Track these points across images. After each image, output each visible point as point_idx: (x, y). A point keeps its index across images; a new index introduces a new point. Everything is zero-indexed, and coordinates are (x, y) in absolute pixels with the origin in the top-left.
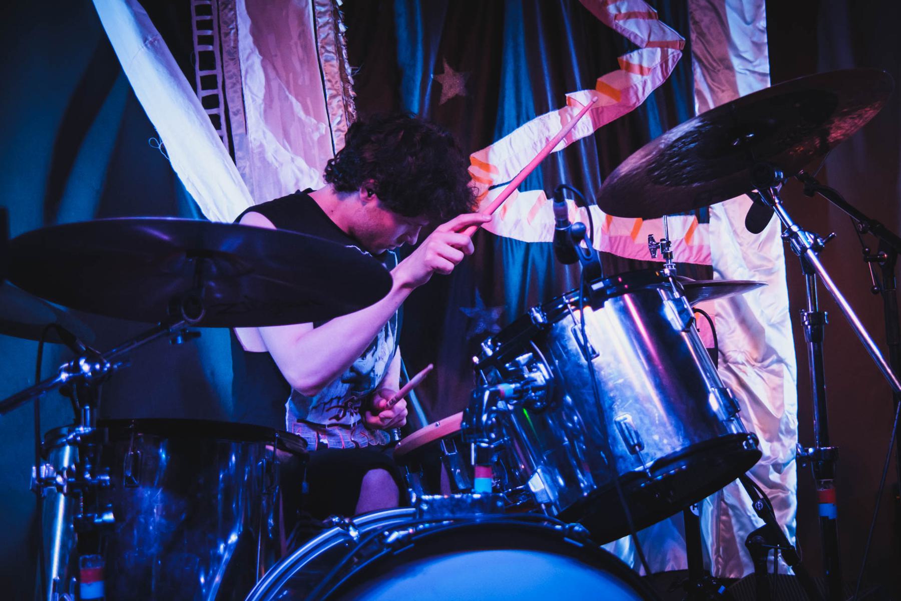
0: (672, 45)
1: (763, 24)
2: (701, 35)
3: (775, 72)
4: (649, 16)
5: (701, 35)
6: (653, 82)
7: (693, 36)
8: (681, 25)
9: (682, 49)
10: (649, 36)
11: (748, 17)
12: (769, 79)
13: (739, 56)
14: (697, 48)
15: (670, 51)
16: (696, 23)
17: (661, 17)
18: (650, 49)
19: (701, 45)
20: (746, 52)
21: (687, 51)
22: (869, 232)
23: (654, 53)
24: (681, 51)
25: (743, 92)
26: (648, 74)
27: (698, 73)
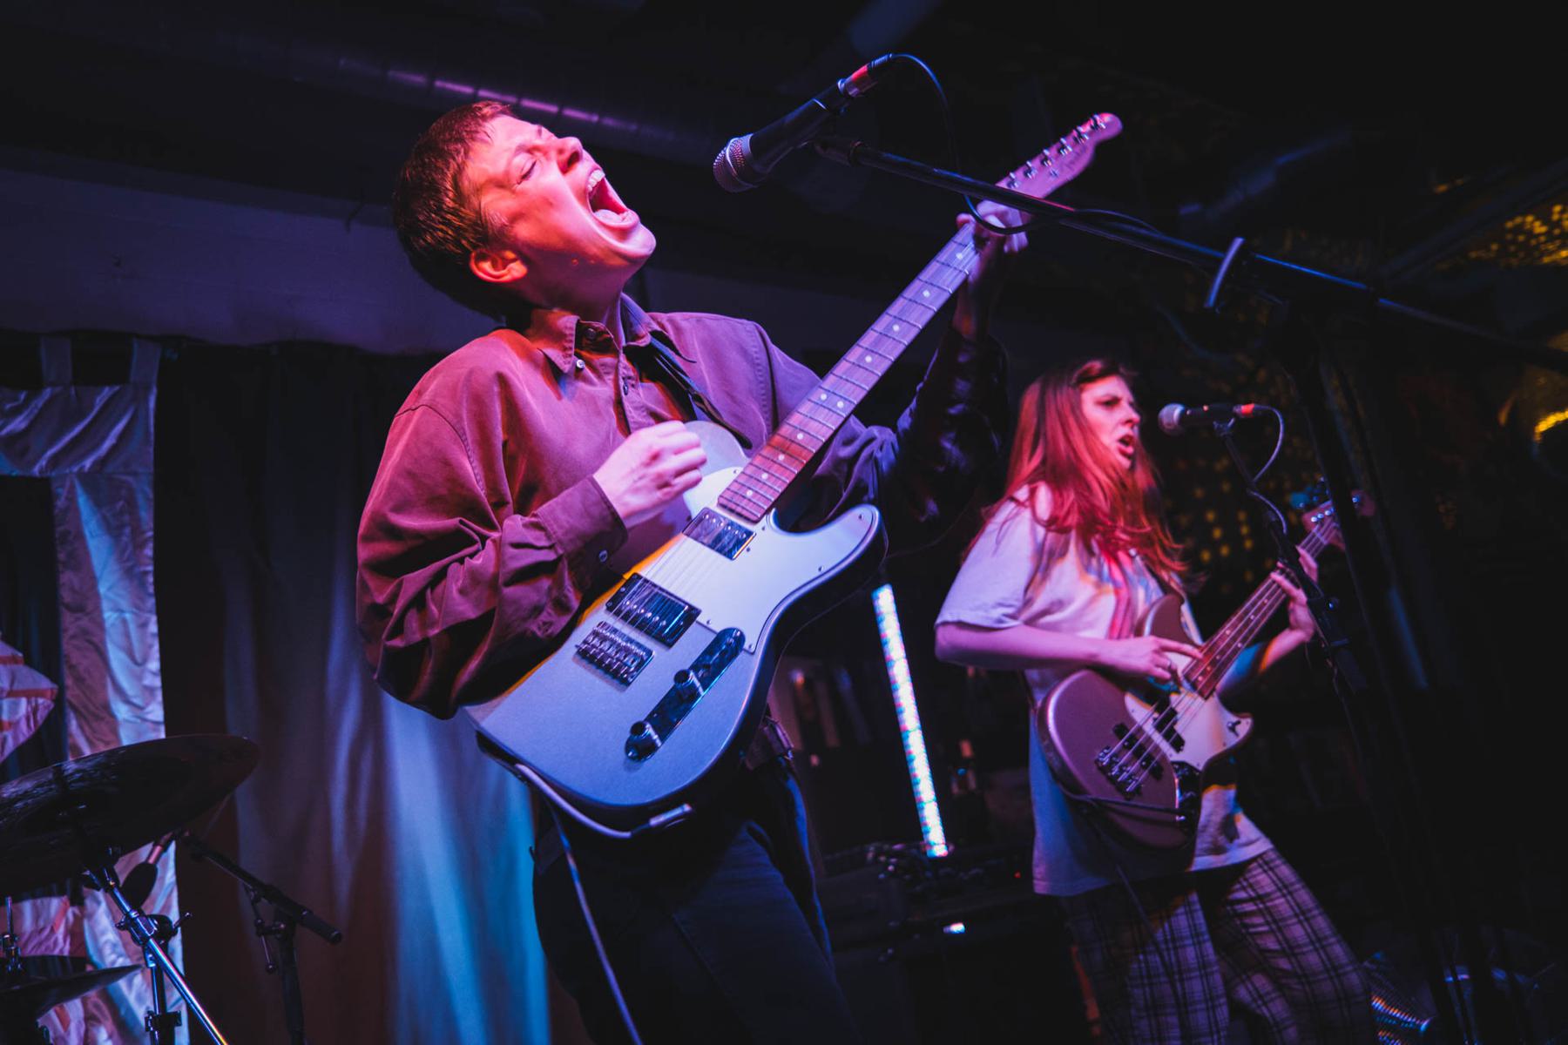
0: (40, 693)
1: (154, 665)
2: (79, 680)
3: (170, 721)
4: (14, 660)
5: (79, 680)
6: (15, 738)
7: (69, 682)
8: (53, 673)
9: (54, 697)
10: (12, 683)
11: (138, 656)
12: (162, 728)
13: (127, 701)
14: (72, 693)
15: (41, 701)
16: (72, 667)
17: (28, 662)
18: (12, 699)
19: (77, 692)
20: (135, 697)
21: (59, 701)
22: (263, 899)
23: (17, 705)
24: (53, 701)
25: (126, 742)
26: (7, 730)
27: (73, 725)
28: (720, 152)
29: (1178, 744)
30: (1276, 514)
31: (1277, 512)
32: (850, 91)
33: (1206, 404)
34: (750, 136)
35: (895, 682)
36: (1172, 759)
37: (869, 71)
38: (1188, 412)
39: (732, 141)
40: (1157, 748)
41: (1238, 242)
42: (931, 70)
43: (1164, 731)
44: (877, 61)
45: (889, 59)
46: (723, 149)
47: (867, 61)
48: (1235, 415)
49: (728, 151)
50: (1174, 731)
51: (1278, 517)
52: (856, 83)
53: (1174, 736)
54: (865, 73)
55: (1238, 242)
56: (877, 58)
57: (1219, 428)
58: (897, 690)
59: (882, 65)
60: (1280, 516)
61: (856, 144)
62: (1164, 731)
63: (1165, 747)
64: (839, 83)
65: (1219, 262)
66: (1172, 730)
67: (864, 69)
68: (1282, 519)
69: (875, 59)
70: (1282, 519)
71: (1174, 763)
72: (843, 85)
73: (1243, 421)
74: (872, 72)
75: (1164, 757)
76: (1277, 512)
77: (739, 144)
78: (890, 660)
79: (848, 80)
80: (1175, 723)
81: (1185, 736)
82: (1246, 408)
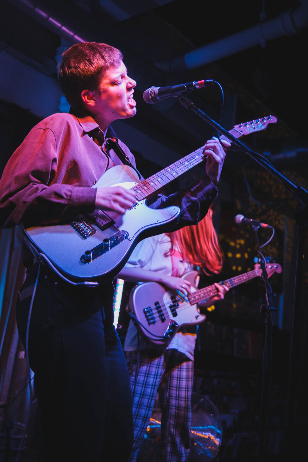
28: (148, 89)
29: (175, 315)
34: (159, 87)
37: (205, 82)
39: (153, 87)
40: (167, 313)
42: (222, 88)
46: (149, 88)
48: (260, 226)
49: (150, 89)
53: (174, 312)
63: (170, 313)
64: (194, 82)
66: (175, 310)
67: (203, 81)
71: (170, 320)
72: (195, 83)
75: (168, 316)
77: (154, 89)
79: (197, 82)
80: (177, 308)
81: (178, 313)
82: (264, 225)
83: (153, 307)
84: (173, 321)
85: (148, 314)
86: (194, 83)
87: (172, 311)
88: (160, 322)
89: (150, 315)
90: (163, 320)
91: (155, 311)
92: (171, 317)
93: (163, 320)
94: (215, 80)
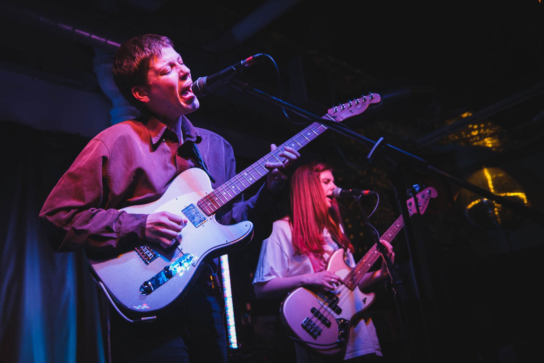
29: (339, 311)
30: (376, 232)
31: (377, 231)
32: (245, 65)
33: (351, 189)
35: (224, 278)
36: (336, 318)
37: (253, 58)
38: (344, 191)
41: (382, 139)
43: (332, 307)
44: (256, 55)
45: (261, 55)
47: (253, 55)
50: (337, 306)
51: (377, 234)
52: (249, 62)
54: (251, 59)
55: (382, 139)
56: (256, 54)
57: (356, 198)
58: (224, 281)
59: (257, 57)
60: (377, 232)
61: (246, 84)
62: (332, 307)
65: (374, 144)
67: (251, 57)
68: (378, 234)
69: (255, 54)
70: (378, 234)
71: (336, 320)
73: (364, 196)
74: (254, 59)
76: (377, 231)
78: (223, 269)
79: (245, 61)
83: (311, 315)
84: (340, 319)
85: (309, 327)
86: (243, 61)
87: (333, 309)
88: (326, 328)
89: (311, 328)
90: (328, 325)
91: (315, 319)
92: (336, 317)
93: (328, 325)
94: (263, 53)
